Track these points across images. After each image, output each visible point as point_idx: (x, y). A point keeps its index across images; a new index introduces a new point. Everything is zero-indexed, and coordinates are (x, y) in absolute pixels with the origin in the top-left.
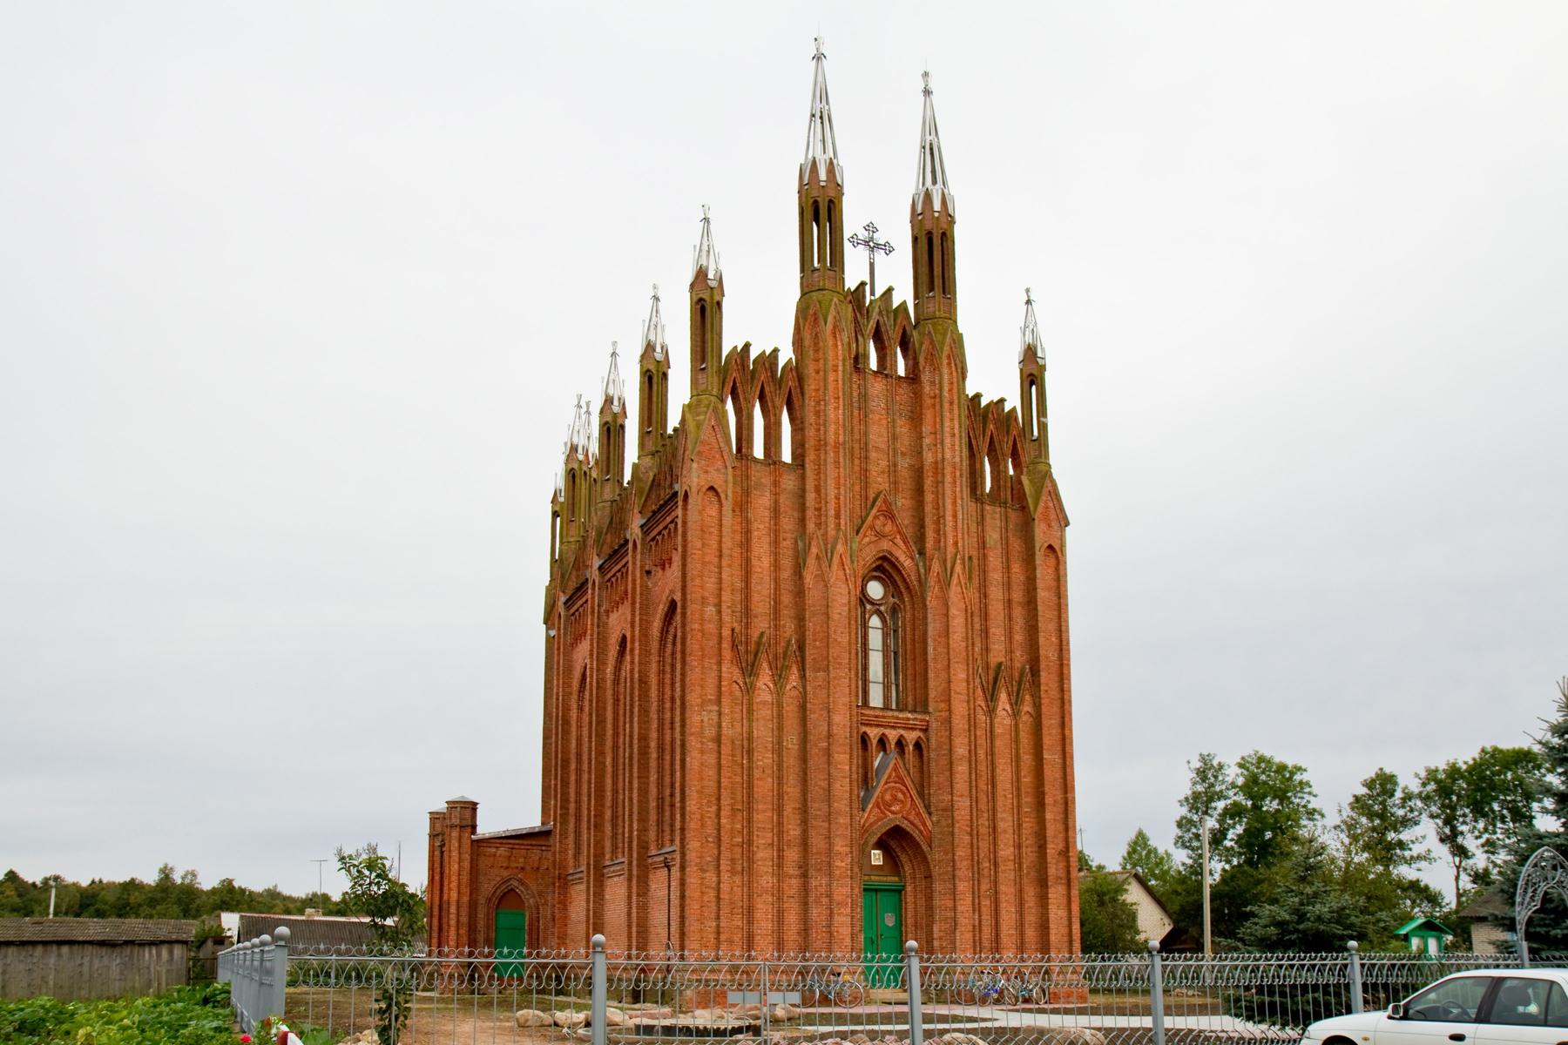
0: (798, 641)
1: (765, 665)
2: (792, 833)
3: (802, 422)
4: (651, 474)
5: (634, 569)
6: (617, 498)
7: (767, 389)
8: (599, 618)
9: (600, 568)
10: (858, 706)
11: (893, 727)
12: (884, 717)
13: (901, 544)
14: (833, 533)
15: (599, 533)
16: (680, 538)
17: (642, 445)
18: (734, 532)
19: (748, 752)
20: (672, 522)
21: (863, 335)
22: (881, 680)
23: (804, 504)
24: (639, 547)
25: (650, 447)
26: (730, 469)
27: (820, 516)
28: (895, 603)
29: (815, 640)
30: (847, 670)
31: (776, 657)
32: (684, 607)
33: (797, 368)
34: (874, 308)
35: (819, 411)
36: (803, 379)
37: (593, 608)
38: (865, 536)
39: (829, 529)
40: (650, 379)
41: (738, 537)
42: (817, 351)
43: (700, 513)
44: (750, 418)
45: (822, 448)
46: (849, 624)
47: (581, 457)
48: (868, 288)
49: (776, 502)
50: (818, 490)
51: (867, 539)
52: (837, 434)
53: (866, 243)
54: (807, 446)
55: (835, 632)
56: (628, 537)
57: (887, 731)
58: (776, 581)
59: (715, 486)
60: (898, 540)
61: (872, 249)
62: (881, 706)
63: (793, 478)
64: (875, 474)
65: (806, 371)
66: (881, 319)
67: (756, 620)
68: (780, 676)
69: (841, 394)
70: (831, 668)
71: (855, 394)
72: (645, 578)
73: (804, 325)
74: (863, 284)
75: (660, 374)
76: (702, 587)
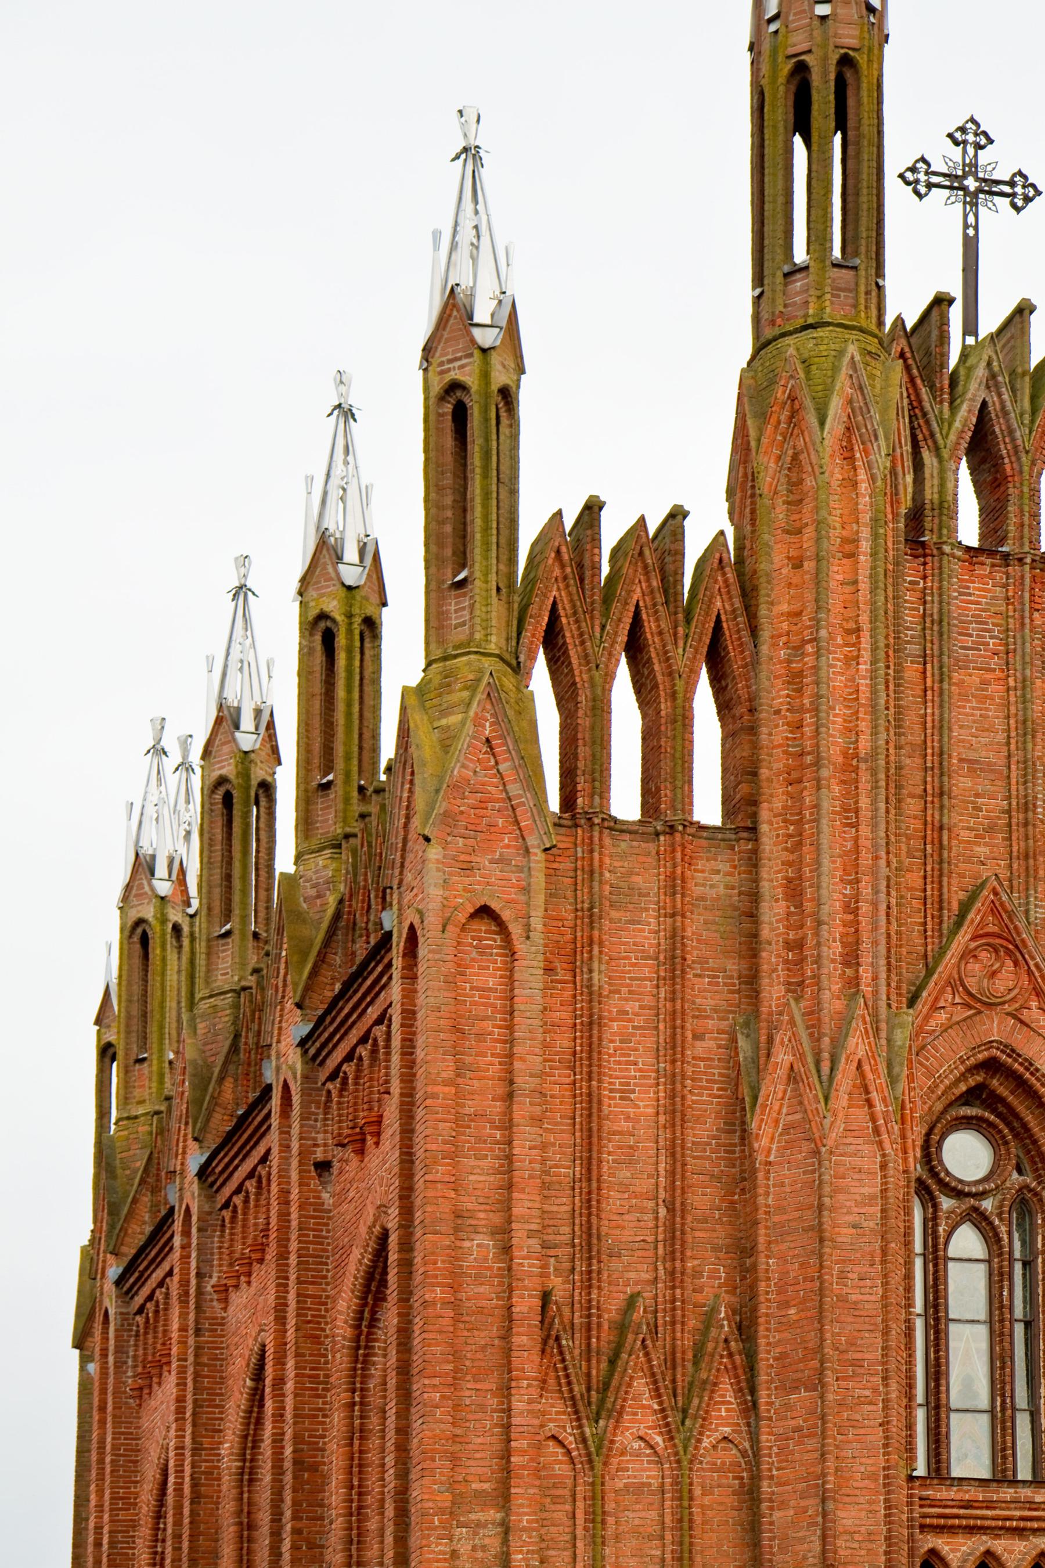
3: (752, 711)
4: (332, 900)
5: (285, 1160)
6: (251, 980)
7: (650, 626)
8: (198, 1308)
9: (203, 1173)
10: (911, 1478)
11: (1019, 1532)
12: (989, 1505)
14: (839, 1005)
15: (201, 1082)
16: (396, 1058)
17: (305, 824)
18: (549, 1027)
20: (379, 1021)
21: (937, 450)
23: (755, 935)
24: (296, 1099)
25: (330, 824)
26: (538, 856)
27: (801, 961)
28: (1027, 1187)
29: (785, 1305)
30: (877, 1380)
31: (672, 1362)
32: (407, 1246)
33: (740, 560)
34: (970, 370)
35: (800, 674)
36: (755, 589)
37: (185, 1283)
39: (826, 995)
40: (329, 639)
41: (563, 1042)
42: (795, 503)
43: (450, 982)
44: (602, 709)
45: (808, 774)
46: (884, 1252)
47: (164, 888)
48: (956, 314)
49: (675, 937)
50: (794, 891)
52: (851, 730)
53: (954, 182)
54: (764, 773)
56: (269, 1075)
57: (1000, 1545)
58: (675, 1151)
59: (494, 905)
61: (972, 200)
62: (985, 1474)
63: (726, 867)
64: (964, 835)
65: (763, 566)
66: (993, 399)
67: (615, 1265)
68: (685, 1411)
69: (864, 618)
70: (830, 1377)
71: (910, 618)
72: (314, 1183)
73: (761, 431)
74: (941, 302)
75: (358, 620)
76: (456, 1185)
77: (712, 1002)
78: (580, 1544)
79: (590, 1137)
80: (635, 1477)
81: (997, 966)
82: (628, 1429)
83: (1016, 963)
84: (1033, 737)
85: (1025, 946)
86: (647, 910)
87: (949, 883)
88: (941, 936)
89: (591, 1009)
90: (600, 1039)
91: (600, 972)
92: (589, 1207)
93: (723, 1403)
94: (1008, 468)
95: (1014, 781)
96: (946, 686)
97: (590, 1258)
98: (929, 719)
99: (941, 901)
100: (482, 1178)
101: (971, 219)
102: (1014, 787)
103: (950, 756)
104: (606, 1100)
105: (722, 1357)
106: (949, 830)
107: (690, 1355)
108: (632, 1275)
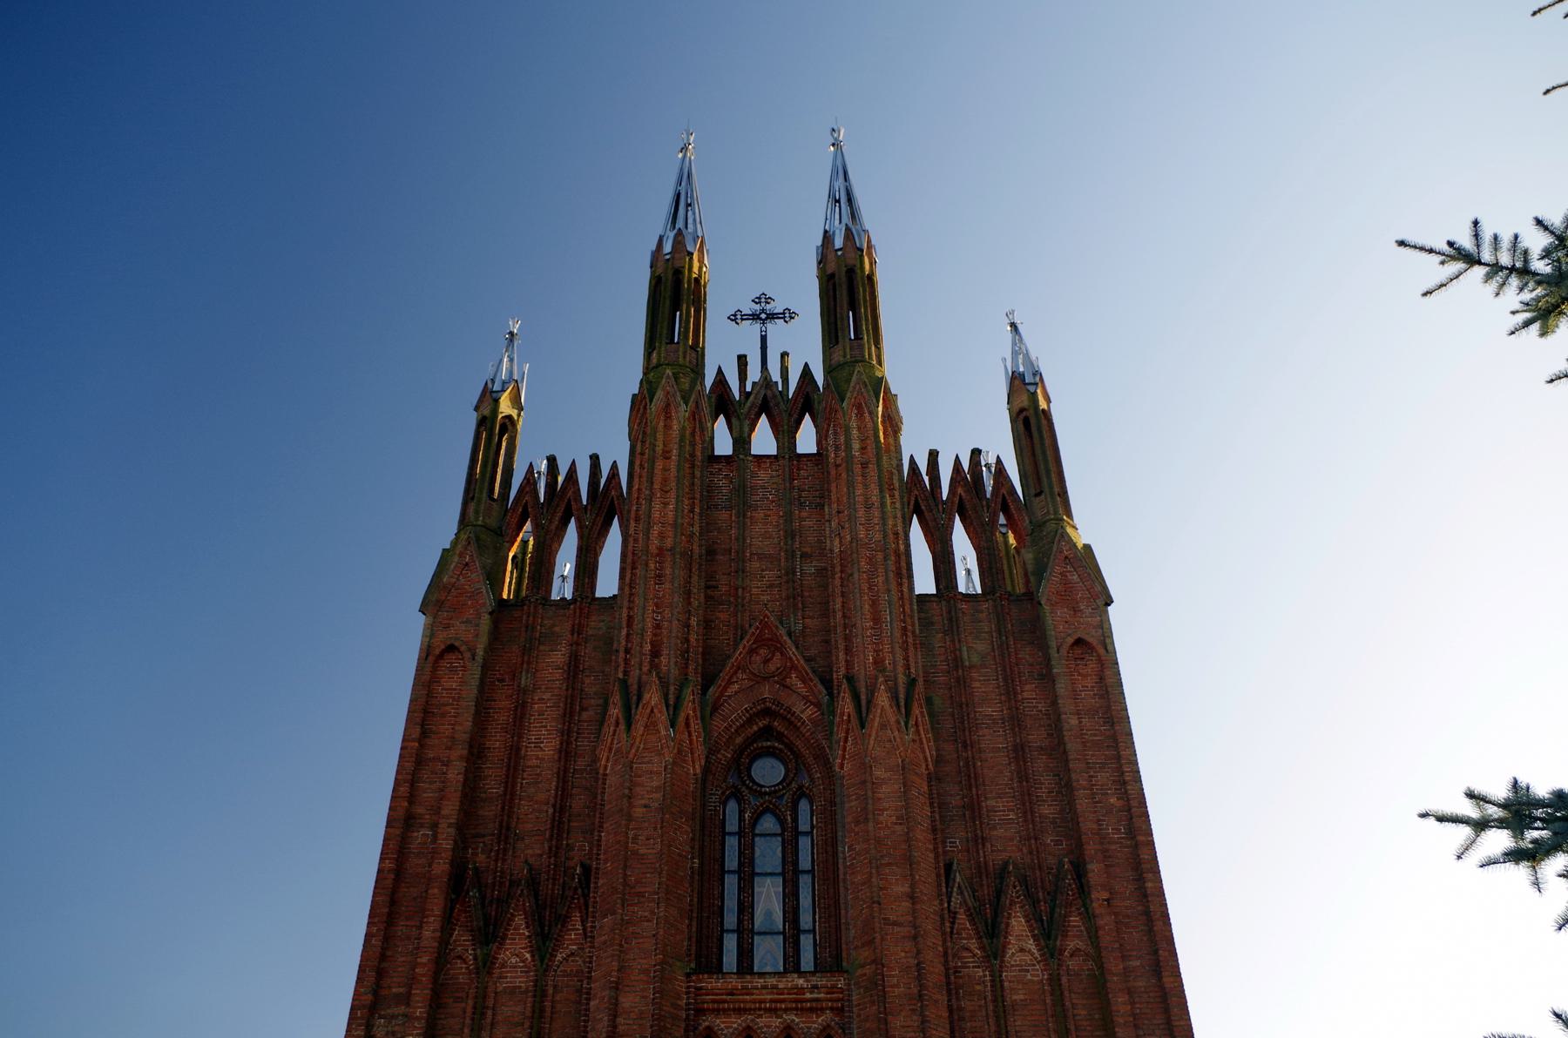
1: (519, 920)
13: (800, 685)
55: (635, 838)
77: (594, 689)
80: (511, 982)
82: (507, 949)
93: (573, 930)
100: (431, 795)
101: (764, 329)
108: (530, 852)
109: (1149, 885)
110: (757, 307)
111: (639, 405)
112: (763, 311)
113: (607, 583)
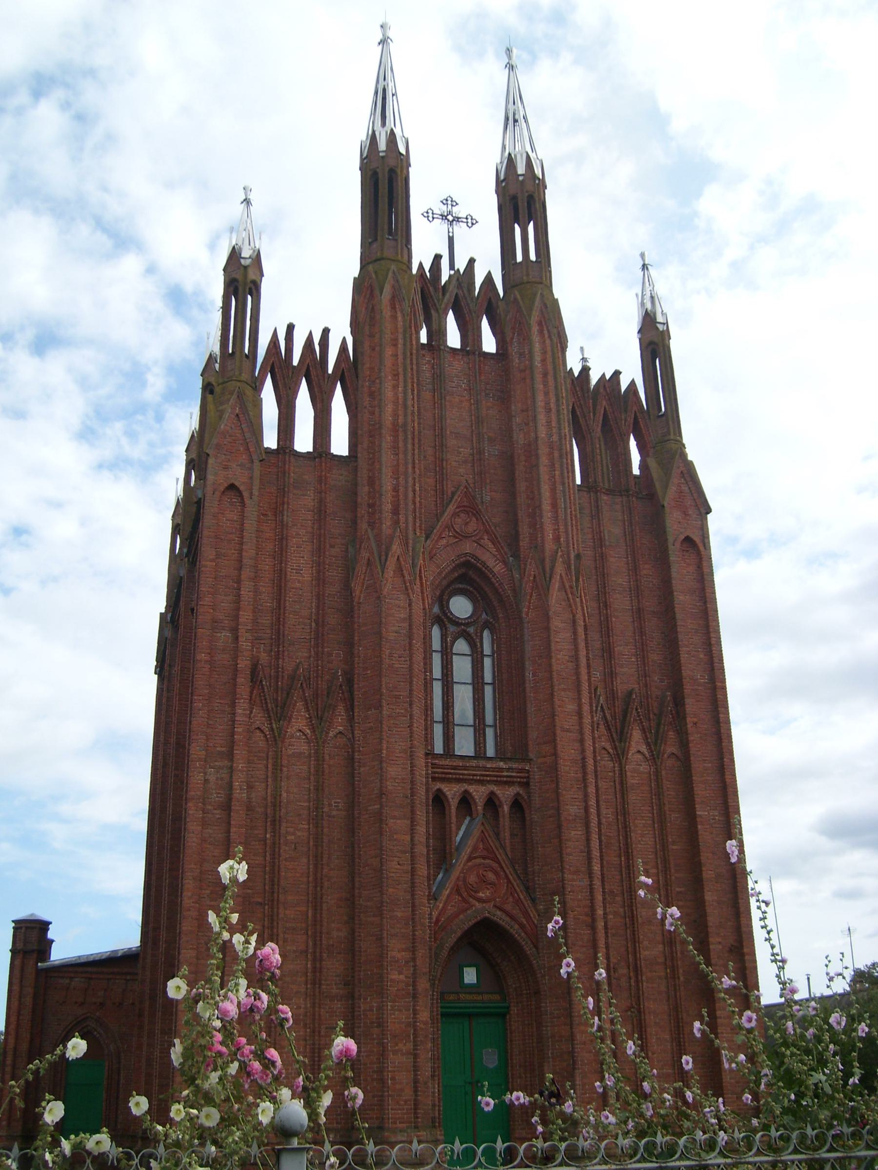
0: (345, 673)
1: (300, 705)
2: (335, 934)
11: (481, 782)
13: (490, 545)
19: (274, 821)
21: (437, 310)
22: (471, 722)
38: (441, 538)
49: (321, 502)
51: (444, 541)
53: (444, 217)
55: (391, 655)
57: (471, 789)
58: (320, 598)
60: (486, 541)
61: (451, 223)
64: (454, 464)
77: (338, 531)
78: (270, 780)
79: (280, 589)
80: (297, 749)
81: (468, 520)
82: (294, 726)
83: (477, 520)
84: (482, 423)
85: (481, 512)
86: (310, 490)
87: (447, 484)
88: (443, 506)
89: (282, 532)
90: (287, 546)
91: (287, 516)
92: (279, 622)
93: (339, 715)
94: (468, 319)
95: (474, 442)
96: (443, 401)
97: (279, 645)
98: (436, 415)
99: (443, 491)
101: (451, 230)
102: (475, 445)
103: (446, 430)
104: (288, 573)
105: (339, 693)
106: (446, 461)
107: (325, 693)
109: (721, 715)
110: (444, 208)
111: (360, 286)
112: (450, 213)
113: (340, 445)
